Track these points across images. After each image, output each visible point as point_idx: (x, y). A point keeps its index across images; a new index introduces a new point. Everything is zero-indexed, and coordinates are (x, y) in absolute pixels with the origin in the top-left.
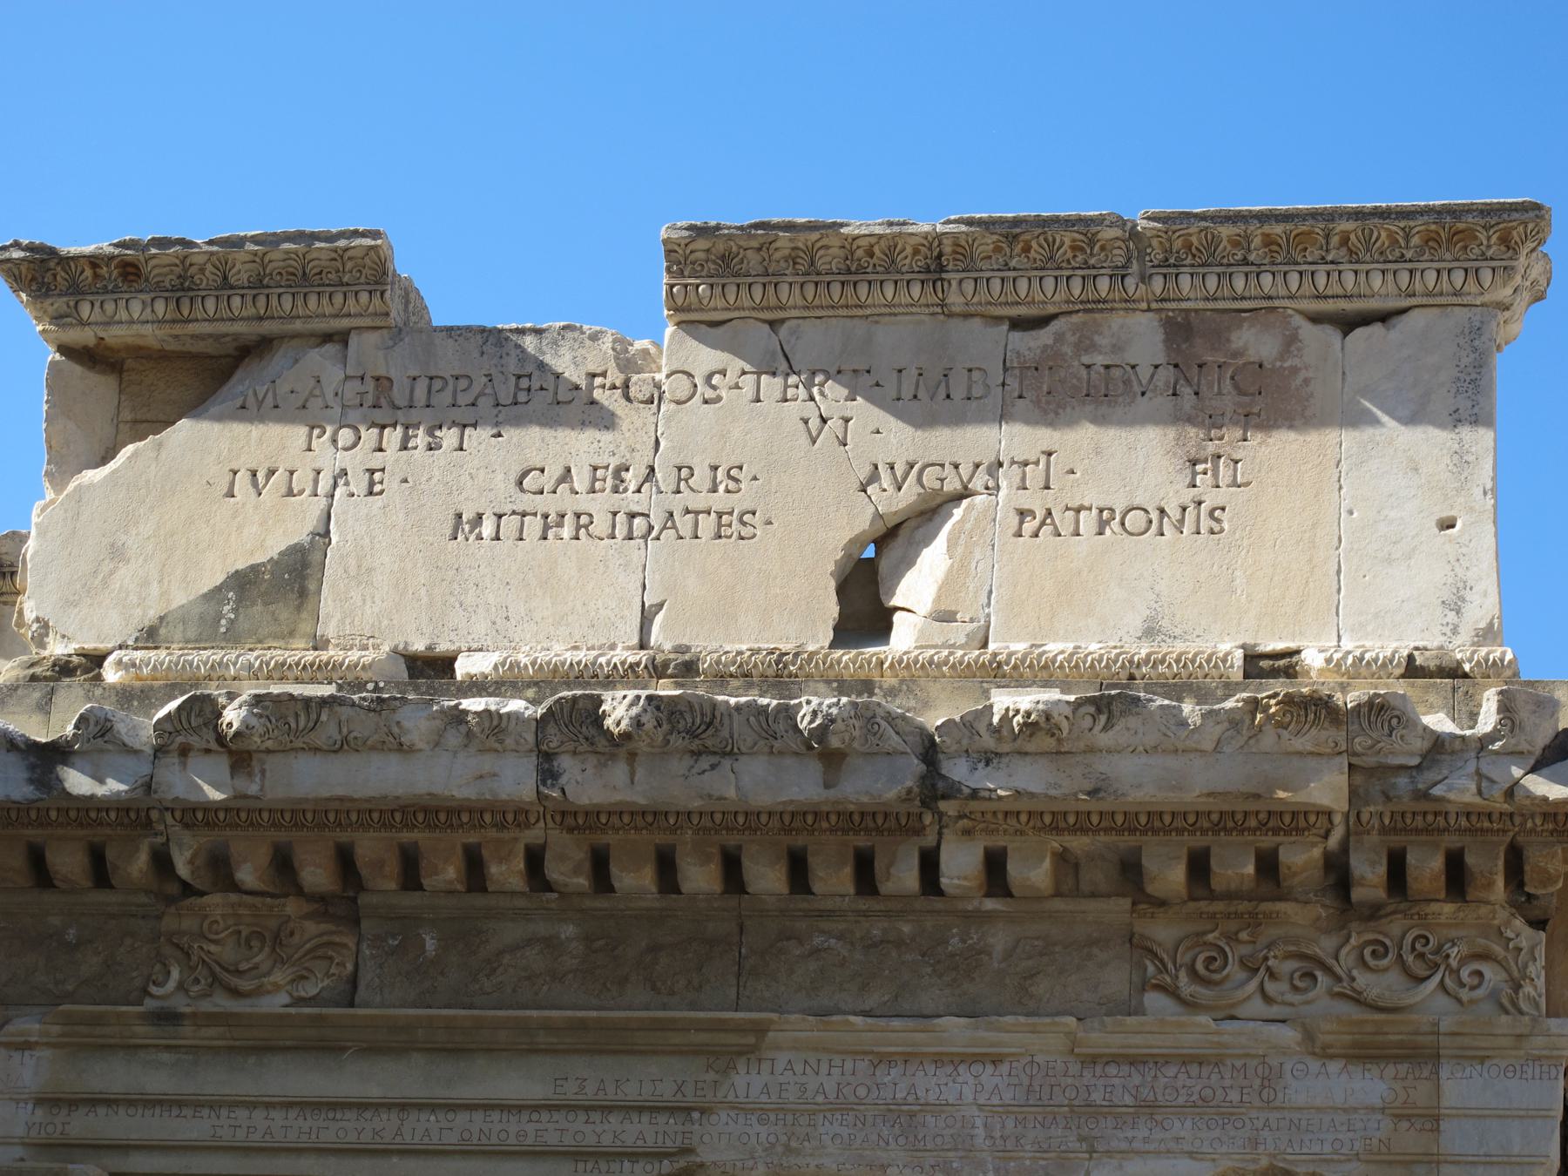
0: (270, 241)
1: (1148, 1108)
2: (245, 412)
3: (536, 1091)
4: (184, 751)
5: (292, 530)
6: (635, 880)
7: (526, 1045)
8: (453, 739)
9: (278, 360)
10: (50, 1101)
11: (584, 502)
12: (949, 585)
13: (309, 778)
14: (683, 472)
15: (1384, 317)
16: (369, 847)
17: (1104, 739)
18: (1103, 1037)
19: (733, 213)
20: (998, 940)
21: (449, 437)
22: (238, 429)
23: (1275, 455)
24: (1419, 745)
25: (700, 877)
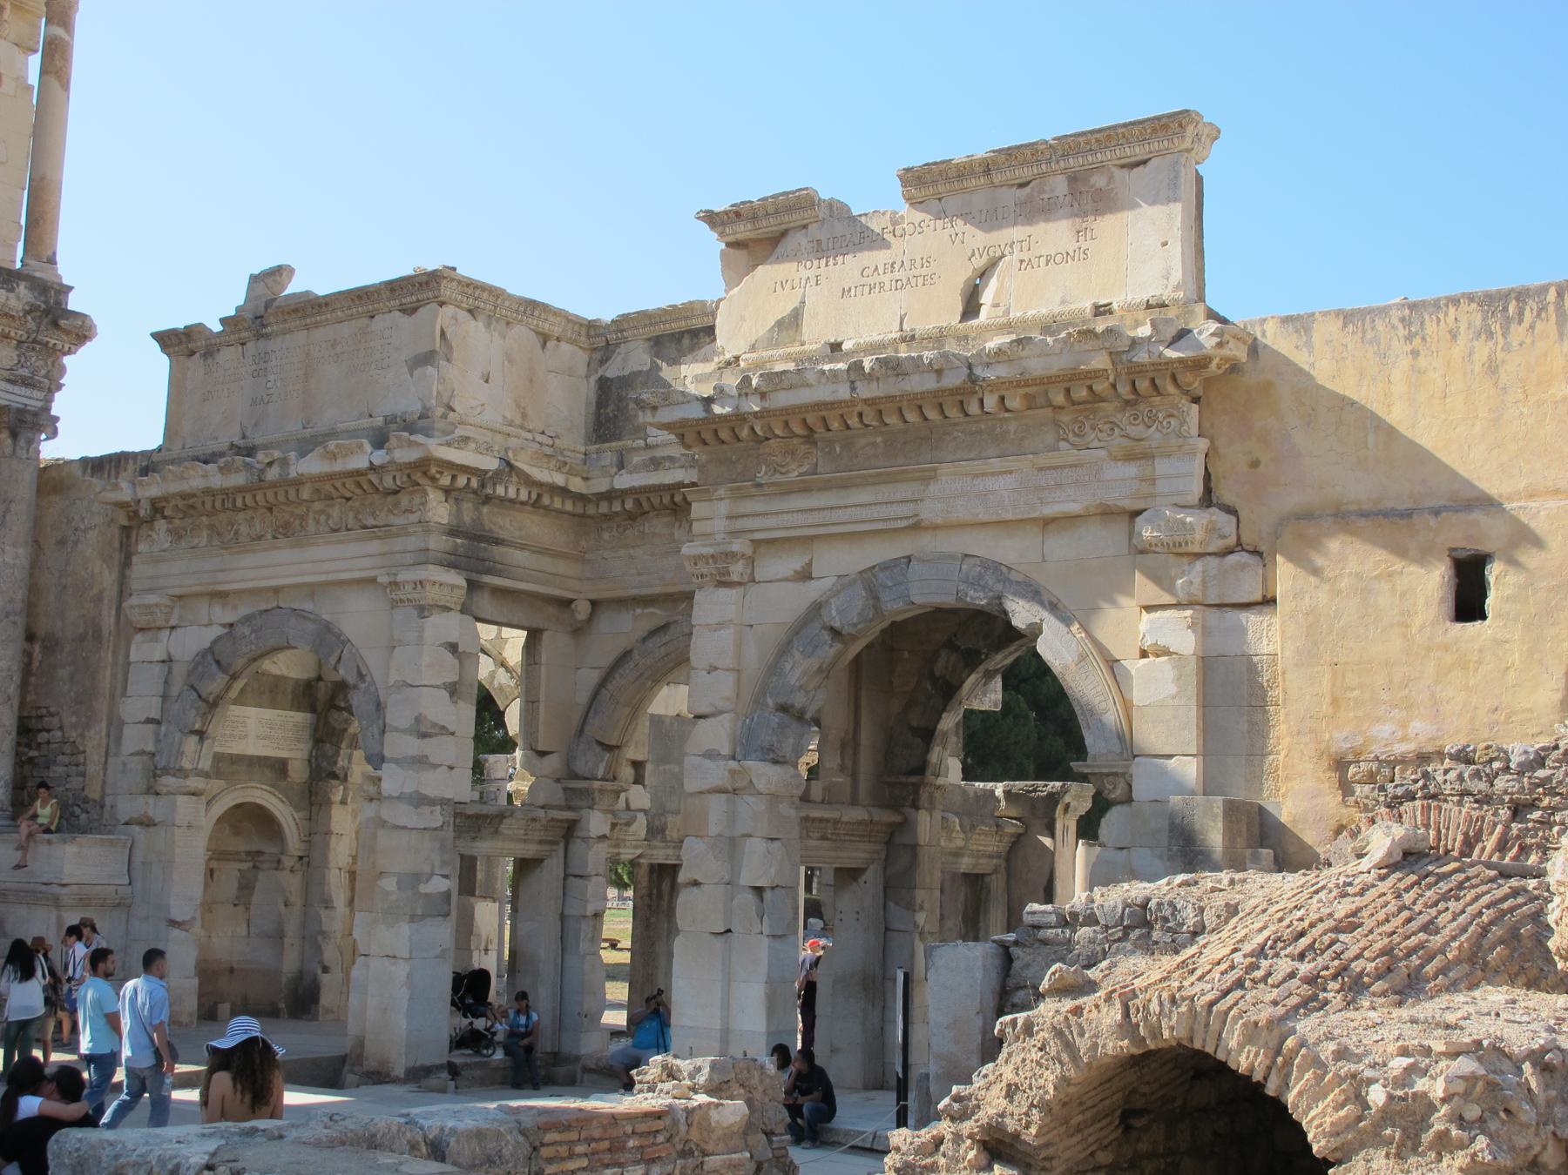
0: (774, 197)
1: (1060, 485)
2: (778, 261)
7: (865, 483)
10: (730, 517)
11: (883, 278)
12: (997, 294)
13: (783, 399)
14: (913, 261)
15: (1144, 162)
18: (1043, 460)
19: (917, 162)
20: (1012, 427)
21: (840, 259)
23: (1106, 224)
24: (1128, 343)
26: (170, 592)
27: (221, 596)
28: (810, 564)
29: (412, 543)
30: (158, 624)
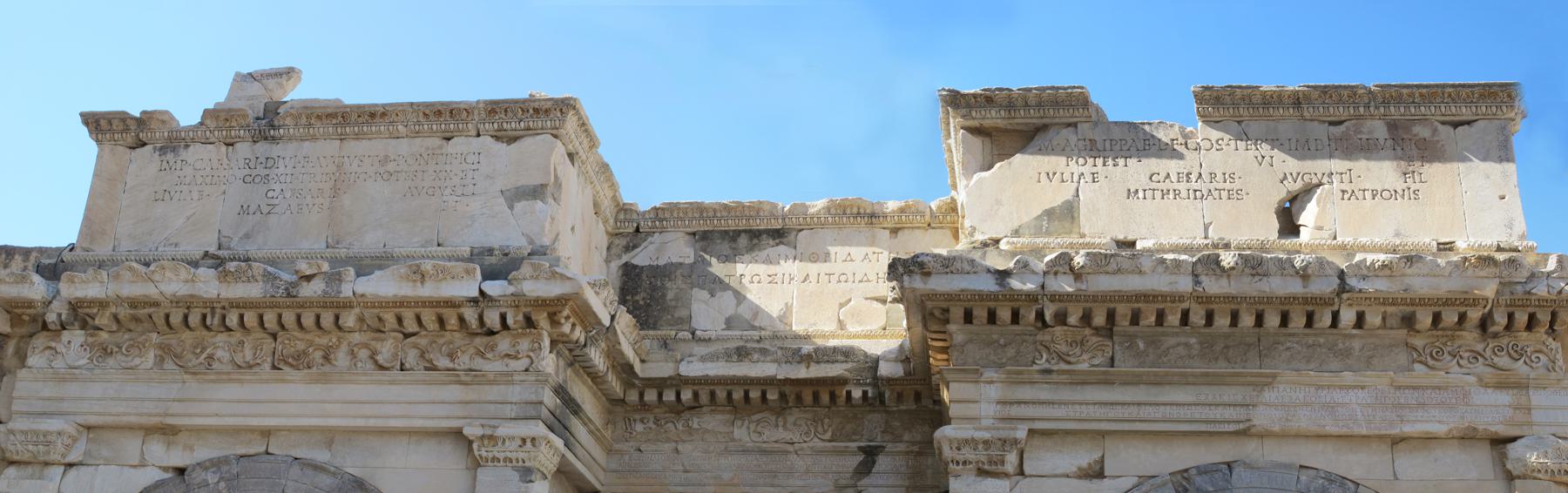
2: (1040, 151)
3: (1190, 399)
4: (1056, 273)
5: (1066, 193)
6: (1222, 321)
7: (1185, 381)
8: (1160, 269)
9: (1051, 132)
11: (1176, 186)
13: (1103, 283)
14: (1213, 176)
15: (1468, 123)
16: (1123, 310)
17: (1409, 271)
18: (1402, 379)
20: (1357, 344)
21: (1121, 161)
22: (1040, 157)
23: (1434, 172)
24: (1526, 274)
25: (1247, 320)
26: (81, 420)
27: (167, 432)
28: (1102, 461)
29: (516, 393)
30: (54, 457)
